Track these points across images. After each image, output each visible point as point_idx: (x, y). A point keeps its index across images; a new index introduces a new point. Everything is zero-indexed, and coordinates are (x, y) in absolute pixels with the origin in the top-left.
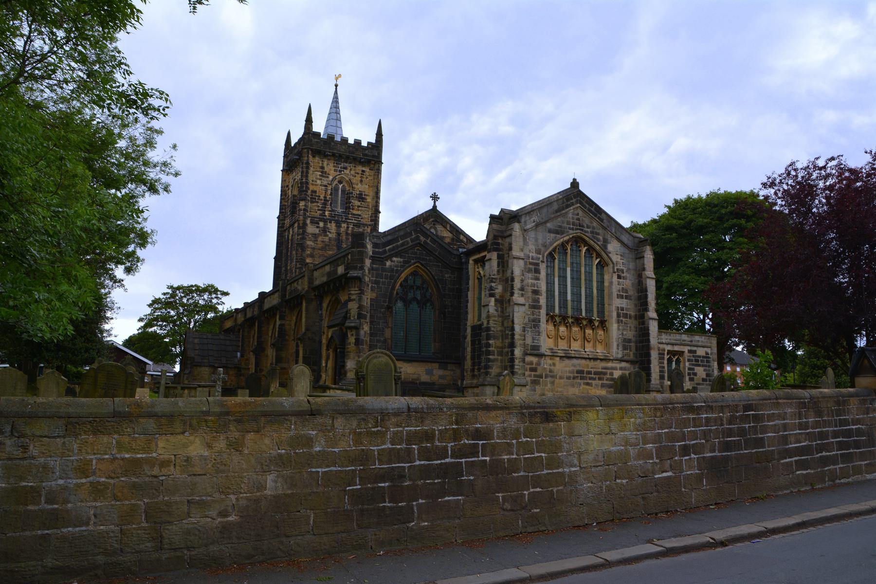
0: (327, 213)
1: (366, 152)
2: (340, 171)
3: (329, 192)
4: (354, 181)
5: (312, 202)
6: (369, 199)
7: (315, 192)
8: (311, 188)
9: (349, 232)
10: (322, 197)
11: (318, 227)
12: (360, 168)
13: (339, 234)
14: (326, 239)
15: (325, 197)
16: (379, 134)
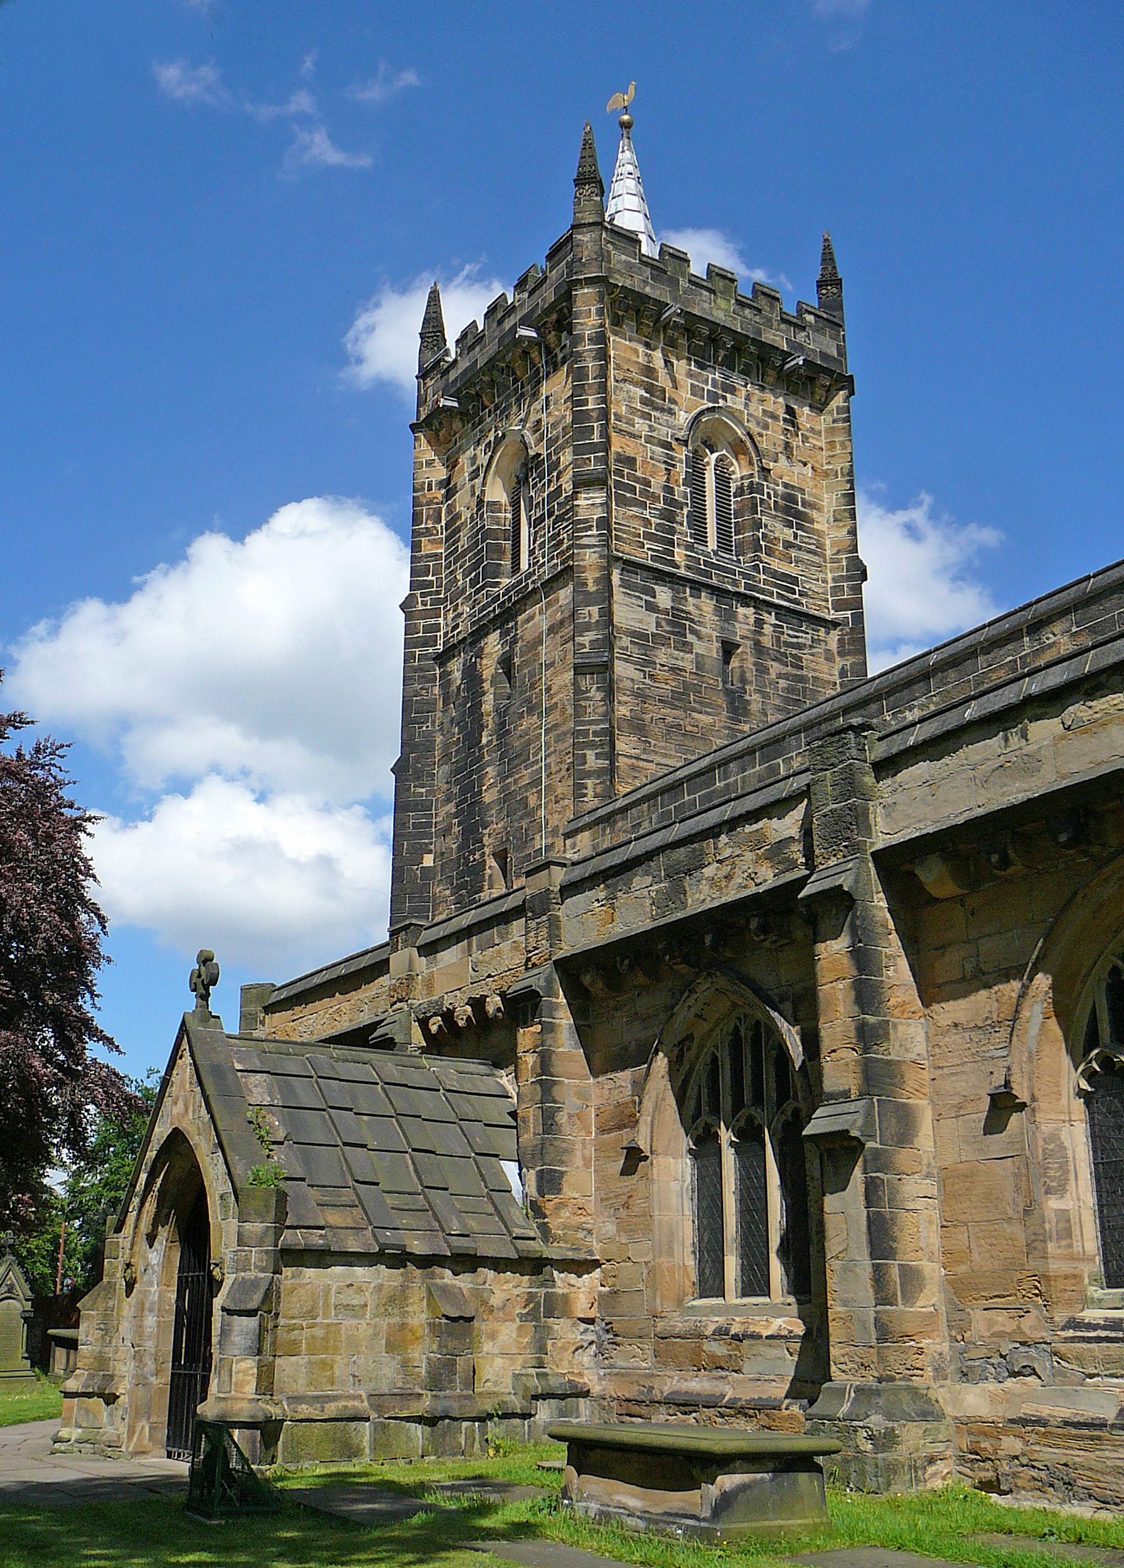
0: (679, 555)
1: (801, 337)
2: (714, 397)
3: (681, 471)
4: (763, 445)
5: (623, 502)
6: (822, 522)
7: (631, 462)
8: (618, 444)
9: (767, 642)
10: (657, 484)
11: (651, 607)
12: (776, 403)
13: (728, 649)
14: (687, 662)
15: (669, 490)
16: (830, 281)
